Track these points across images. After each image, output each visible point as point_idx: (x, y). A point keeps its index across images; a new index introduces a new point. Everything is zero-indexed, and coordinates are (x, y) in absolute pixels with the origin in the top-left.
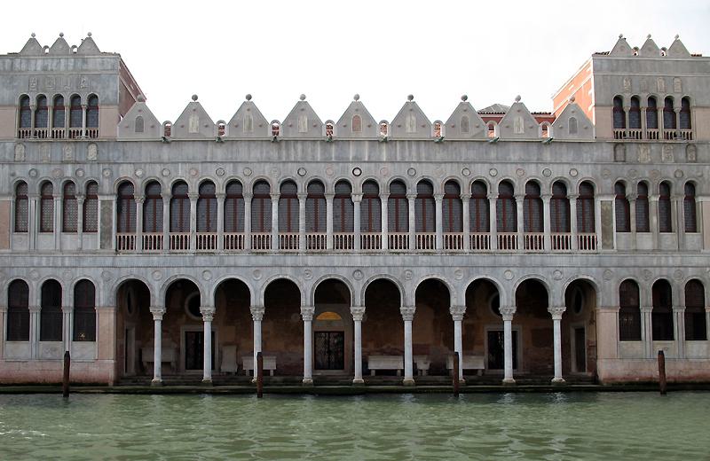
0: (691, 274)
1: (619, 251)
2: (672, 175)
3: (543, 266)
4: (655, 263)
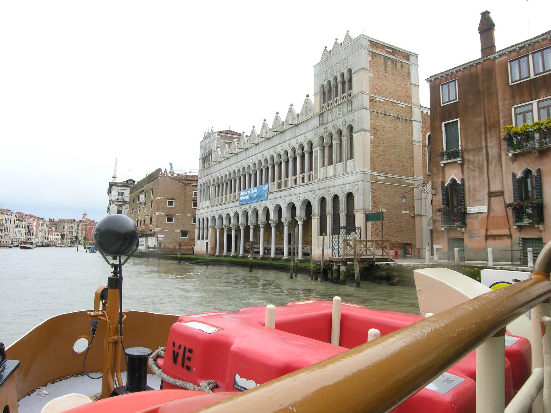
0: (348, 189)
1: (320, 180)
2: (341, 124)
3: (294, 194)
4: (332, 185)
